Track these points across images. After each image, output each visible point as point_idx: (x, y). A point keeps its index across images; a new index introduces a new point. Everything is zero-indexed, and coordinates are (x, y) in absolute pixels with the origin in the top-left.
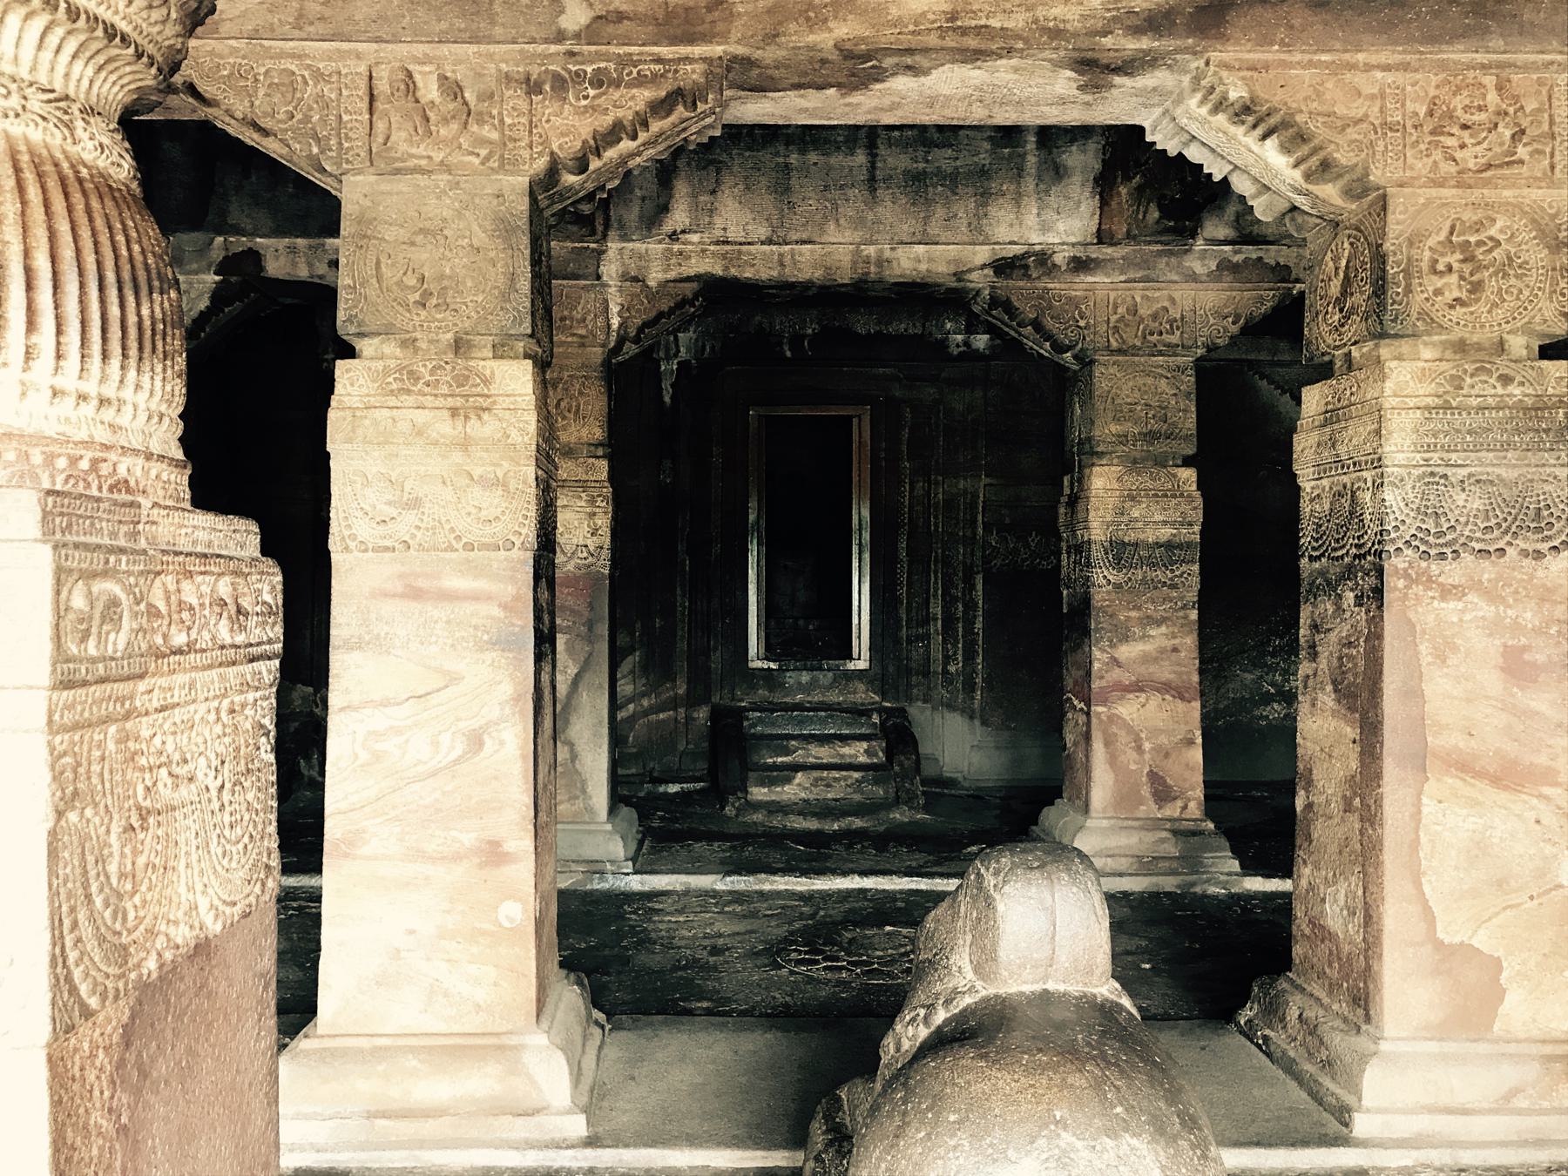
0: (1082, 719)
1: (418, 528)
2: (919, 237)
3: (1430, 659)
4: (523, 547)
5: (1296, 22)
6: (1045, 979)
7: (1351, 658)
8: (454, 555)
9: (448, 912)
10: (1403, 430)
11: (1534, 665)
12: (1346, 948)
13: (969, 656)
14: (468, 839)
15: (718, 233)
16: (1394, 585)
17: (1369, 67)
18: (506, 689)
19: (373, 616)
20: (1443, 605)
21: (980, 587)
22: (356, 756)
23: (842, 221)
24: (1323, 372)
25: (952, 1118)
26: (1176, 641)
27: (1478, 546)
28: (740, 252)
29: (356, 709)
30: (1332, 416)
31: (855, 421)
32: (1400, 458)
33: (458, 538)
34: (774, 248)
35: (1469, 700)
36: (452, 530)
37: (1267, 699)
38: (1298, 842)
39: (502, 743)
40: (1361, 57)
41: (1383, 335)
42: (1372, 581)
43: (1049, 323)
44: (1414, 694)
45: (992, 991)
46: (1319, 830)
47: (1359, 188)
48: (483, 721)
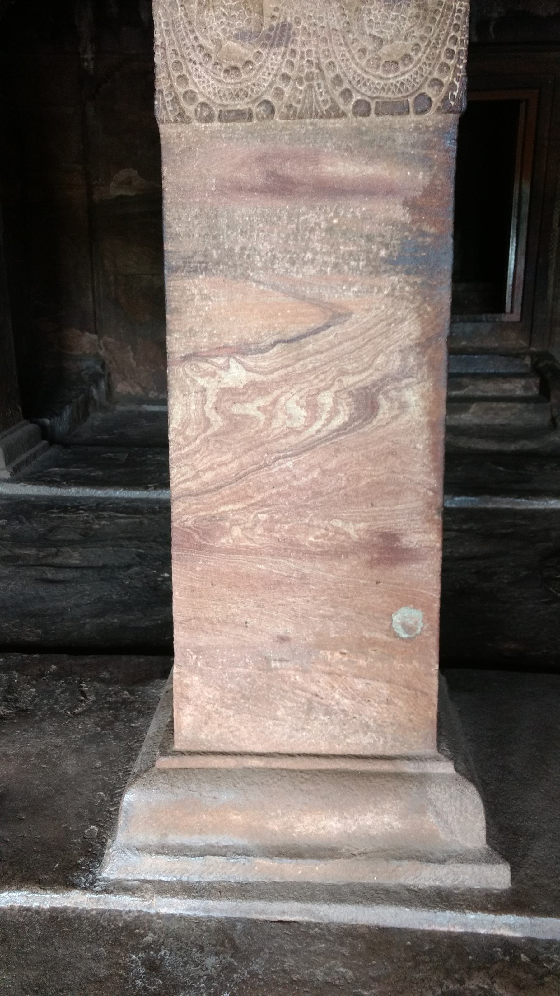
1: (286, 78)
4: (445, 108)
8: (339, 123)
9: (330, 618)
14: (355, 530)
18: (410, 329)
19: (223, 222)
22: (208, 423)
29: (205, 358)
33: (347, 94)
36: (338, 80)
39: (403, 406)
48: (377, 376)
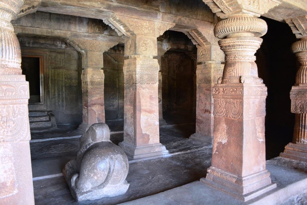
0: (86, 110)
2: (58, 29)
5: (126, 11)
6: (102, 140)
7: (132, 97)
11: (153, 98)
12: (132, 136)
13: (63, 101)
15: (21, 24)
16: (138, 87)
17: (134, 18)
21: (64, 89)
23: (45, 25)
24: (128, 58)
25: (97, 156)
26: (101, 97)
27: (147, 82)
28: (25, 28)
30: (129, 65)
31: (40, 59)
32: (138, 71)
34: (32, 28)
35: (146, 102)
37: (110, 106)
38: (124, 123)
40: (133, 17)
41: (136, 54)
42: (135, 87)
43: (80, 45)
44: (140, 102)
45: (95, 142)
46: (128, 121)
47: (133, 34)
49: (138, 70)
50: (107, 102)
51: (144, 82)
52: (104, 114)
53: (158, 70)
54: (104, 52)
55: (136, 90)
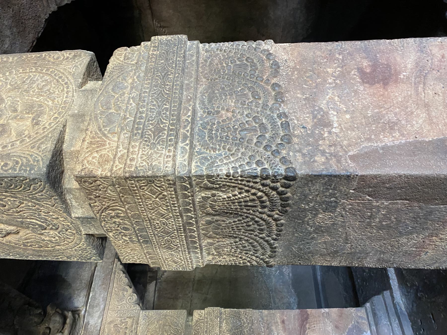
3: (397, 134)
10: (150, 157)
11: (375, 66)
16: (320, 165)
20: (336, 125)
26: (279, 321)
49: (172, 160)
50: (274, 280)
51: (274, 124)
52: (334, 311)
53: (180, 41)
54: (138, 307)
55: (348, 178)
